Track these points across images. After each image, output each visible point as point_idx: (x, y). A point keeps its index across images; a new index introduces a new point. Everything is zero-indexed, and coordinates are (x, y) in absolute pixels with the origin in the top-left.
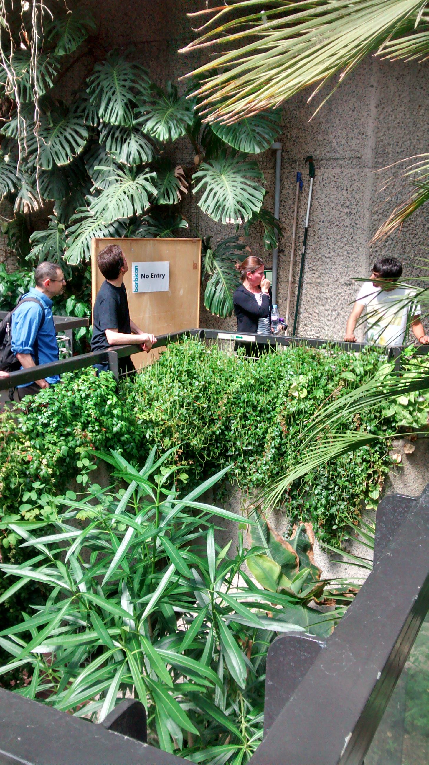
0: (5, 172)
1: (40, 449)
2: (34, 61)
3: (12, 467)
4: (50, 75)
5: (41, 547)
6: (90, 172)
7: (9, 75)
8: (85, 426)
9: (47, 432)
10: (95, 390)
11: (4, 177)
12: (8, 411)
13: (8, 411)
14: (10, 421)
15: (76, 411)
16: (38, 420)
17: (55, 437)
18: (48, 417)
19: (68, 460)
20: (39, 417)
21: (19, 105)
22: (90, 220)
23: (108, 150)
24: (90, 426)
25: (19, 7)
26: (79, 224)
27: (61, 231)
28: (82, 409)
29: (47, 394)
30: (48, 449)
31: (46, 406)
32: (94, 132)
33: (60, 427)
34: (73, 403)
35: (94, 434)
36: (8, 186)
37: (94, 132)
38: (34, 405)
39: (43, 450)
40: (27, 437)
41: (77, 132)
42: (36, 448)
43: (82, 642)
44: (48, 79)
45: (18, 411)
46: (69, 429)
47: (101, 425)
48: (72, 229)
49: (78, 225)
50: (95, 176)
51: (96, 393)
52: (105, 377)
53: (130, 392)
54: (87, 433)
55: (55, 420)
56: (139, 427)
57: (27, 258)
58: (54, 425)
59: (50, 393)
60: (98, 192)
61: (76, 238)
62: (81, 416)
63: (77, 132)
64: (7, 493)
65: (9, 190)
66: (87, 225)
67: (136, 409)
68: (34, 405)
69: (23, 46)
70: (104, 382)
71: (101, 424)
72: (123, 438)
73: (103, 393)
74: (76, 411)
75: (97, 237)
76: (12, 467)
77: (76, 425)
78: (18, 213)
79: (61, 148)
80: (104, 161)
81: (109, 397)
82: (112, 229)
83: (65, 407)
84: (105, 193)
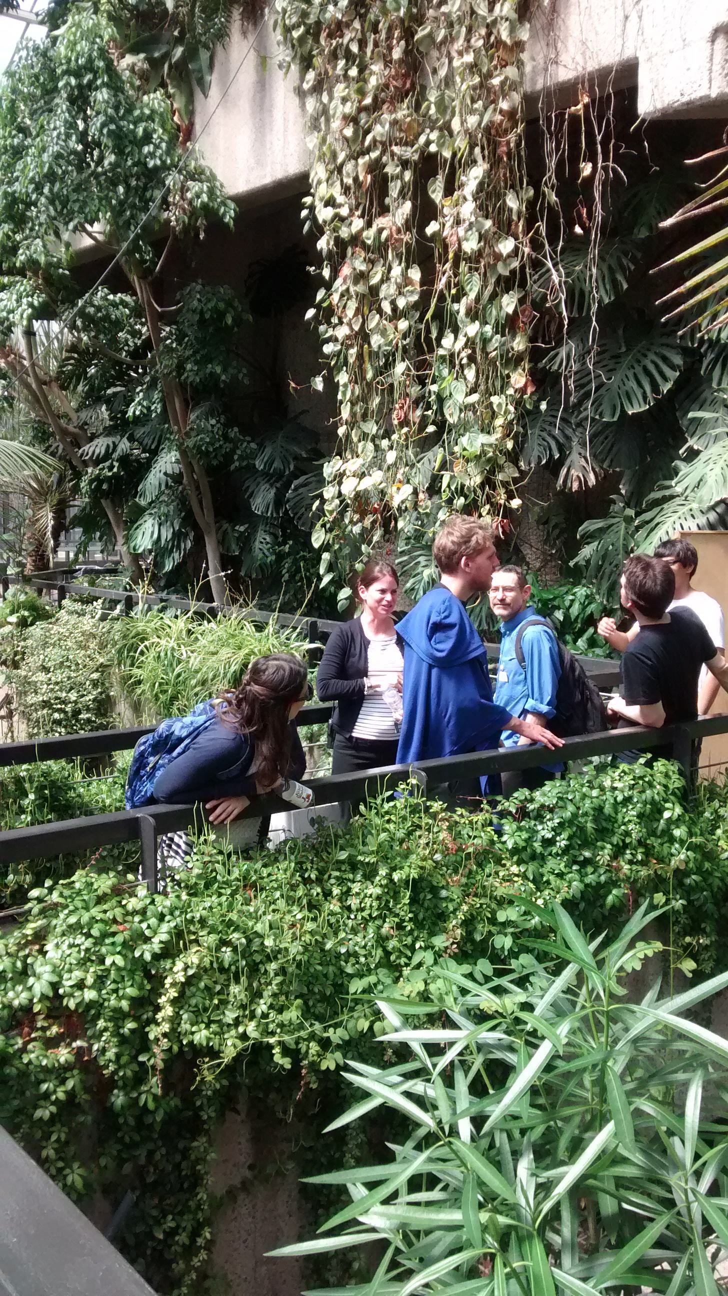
0: (548, 428)
1: (534, 881)
2: (594, 252)
3: (481, 904)
4: (623, 269)
5: (417, 1048)
6: (684, 423)
7: (555, 277)
8: (618, 852)
9: (550, 854)
10: (643, 791)
11: (545, 434)
12: (487, 811)
13: (487, 811)
14: (489, 829)
15: (605, 823)
16: (537, 832)
17: (563, 864)
18: (553, 829)
19: (582, 905)
20: (540, 827)
21: (566, 323)
22: (678, 501)
23: (714, 385)
24: (628, 852)
25: (576, 172)
26: (659, 508)
27: (629, 520)
28: (616, 822)
29: (555, 791)
30: (548, 882)
31: (551, 810)
32: (693, 357)
33: (574, 848)
34: (599, 809)
35: (634, 867)
36: (550, 450)
37: (693, 357)
38: (531, 807)
39: (539, 883)
40: (515, 858)
41: (665, 359)
42: (528, 879)
43: (441, 1224)
44: (620, 277)
45: (503, 814)
46: (587, 854)
47: (647, 854)
48: (647, 516)
49: (656, 510)
50: (692, 429)
51: (644, 797)
52: (662, 769)
53: (711, 800)
54: (623, 863)
55: (565, 835)
56: (722, 863)
57: (571, 564)
58: (563, 843)
59: (560, 789)
60: (693, 454)
61: (652, 530)
62: (614, 833)
63: (665, 359)
64: (469, 947)
65: (551, 455)
66: (671, 510)
67: (719, 832)
68: (531, 807)
69: (578, 230)
70: (659, 778)
71: (649, 852)
72: (688, 881)
73: (656, 797)
74: (605, 823)
75: (686, 530)
76: (481, 904)
77: (603, 848)
78: (562, 491)
79: (635, 386)
80: (708, 402)
81: (667, 805)
82: (712, 516)
83: (586, 814)
84: (703, 457)
